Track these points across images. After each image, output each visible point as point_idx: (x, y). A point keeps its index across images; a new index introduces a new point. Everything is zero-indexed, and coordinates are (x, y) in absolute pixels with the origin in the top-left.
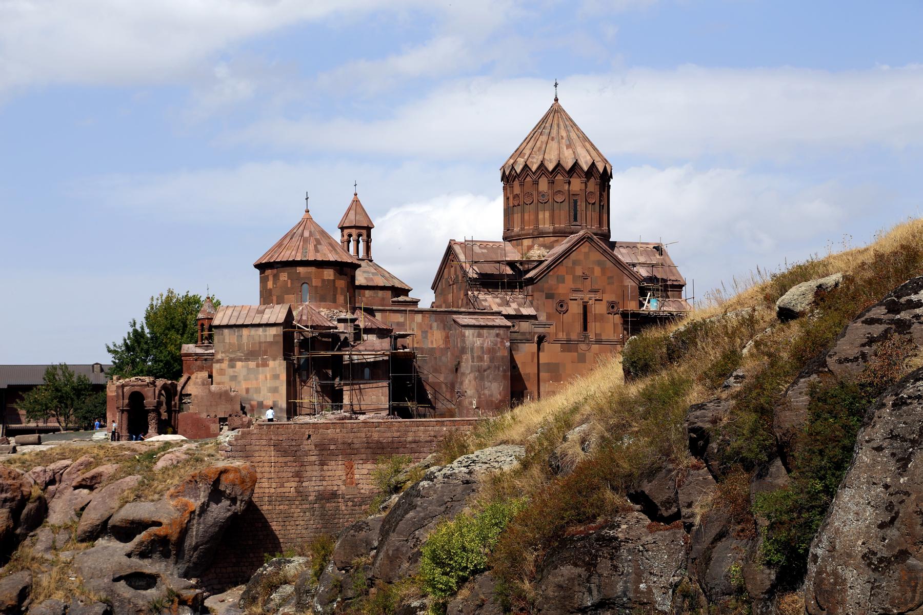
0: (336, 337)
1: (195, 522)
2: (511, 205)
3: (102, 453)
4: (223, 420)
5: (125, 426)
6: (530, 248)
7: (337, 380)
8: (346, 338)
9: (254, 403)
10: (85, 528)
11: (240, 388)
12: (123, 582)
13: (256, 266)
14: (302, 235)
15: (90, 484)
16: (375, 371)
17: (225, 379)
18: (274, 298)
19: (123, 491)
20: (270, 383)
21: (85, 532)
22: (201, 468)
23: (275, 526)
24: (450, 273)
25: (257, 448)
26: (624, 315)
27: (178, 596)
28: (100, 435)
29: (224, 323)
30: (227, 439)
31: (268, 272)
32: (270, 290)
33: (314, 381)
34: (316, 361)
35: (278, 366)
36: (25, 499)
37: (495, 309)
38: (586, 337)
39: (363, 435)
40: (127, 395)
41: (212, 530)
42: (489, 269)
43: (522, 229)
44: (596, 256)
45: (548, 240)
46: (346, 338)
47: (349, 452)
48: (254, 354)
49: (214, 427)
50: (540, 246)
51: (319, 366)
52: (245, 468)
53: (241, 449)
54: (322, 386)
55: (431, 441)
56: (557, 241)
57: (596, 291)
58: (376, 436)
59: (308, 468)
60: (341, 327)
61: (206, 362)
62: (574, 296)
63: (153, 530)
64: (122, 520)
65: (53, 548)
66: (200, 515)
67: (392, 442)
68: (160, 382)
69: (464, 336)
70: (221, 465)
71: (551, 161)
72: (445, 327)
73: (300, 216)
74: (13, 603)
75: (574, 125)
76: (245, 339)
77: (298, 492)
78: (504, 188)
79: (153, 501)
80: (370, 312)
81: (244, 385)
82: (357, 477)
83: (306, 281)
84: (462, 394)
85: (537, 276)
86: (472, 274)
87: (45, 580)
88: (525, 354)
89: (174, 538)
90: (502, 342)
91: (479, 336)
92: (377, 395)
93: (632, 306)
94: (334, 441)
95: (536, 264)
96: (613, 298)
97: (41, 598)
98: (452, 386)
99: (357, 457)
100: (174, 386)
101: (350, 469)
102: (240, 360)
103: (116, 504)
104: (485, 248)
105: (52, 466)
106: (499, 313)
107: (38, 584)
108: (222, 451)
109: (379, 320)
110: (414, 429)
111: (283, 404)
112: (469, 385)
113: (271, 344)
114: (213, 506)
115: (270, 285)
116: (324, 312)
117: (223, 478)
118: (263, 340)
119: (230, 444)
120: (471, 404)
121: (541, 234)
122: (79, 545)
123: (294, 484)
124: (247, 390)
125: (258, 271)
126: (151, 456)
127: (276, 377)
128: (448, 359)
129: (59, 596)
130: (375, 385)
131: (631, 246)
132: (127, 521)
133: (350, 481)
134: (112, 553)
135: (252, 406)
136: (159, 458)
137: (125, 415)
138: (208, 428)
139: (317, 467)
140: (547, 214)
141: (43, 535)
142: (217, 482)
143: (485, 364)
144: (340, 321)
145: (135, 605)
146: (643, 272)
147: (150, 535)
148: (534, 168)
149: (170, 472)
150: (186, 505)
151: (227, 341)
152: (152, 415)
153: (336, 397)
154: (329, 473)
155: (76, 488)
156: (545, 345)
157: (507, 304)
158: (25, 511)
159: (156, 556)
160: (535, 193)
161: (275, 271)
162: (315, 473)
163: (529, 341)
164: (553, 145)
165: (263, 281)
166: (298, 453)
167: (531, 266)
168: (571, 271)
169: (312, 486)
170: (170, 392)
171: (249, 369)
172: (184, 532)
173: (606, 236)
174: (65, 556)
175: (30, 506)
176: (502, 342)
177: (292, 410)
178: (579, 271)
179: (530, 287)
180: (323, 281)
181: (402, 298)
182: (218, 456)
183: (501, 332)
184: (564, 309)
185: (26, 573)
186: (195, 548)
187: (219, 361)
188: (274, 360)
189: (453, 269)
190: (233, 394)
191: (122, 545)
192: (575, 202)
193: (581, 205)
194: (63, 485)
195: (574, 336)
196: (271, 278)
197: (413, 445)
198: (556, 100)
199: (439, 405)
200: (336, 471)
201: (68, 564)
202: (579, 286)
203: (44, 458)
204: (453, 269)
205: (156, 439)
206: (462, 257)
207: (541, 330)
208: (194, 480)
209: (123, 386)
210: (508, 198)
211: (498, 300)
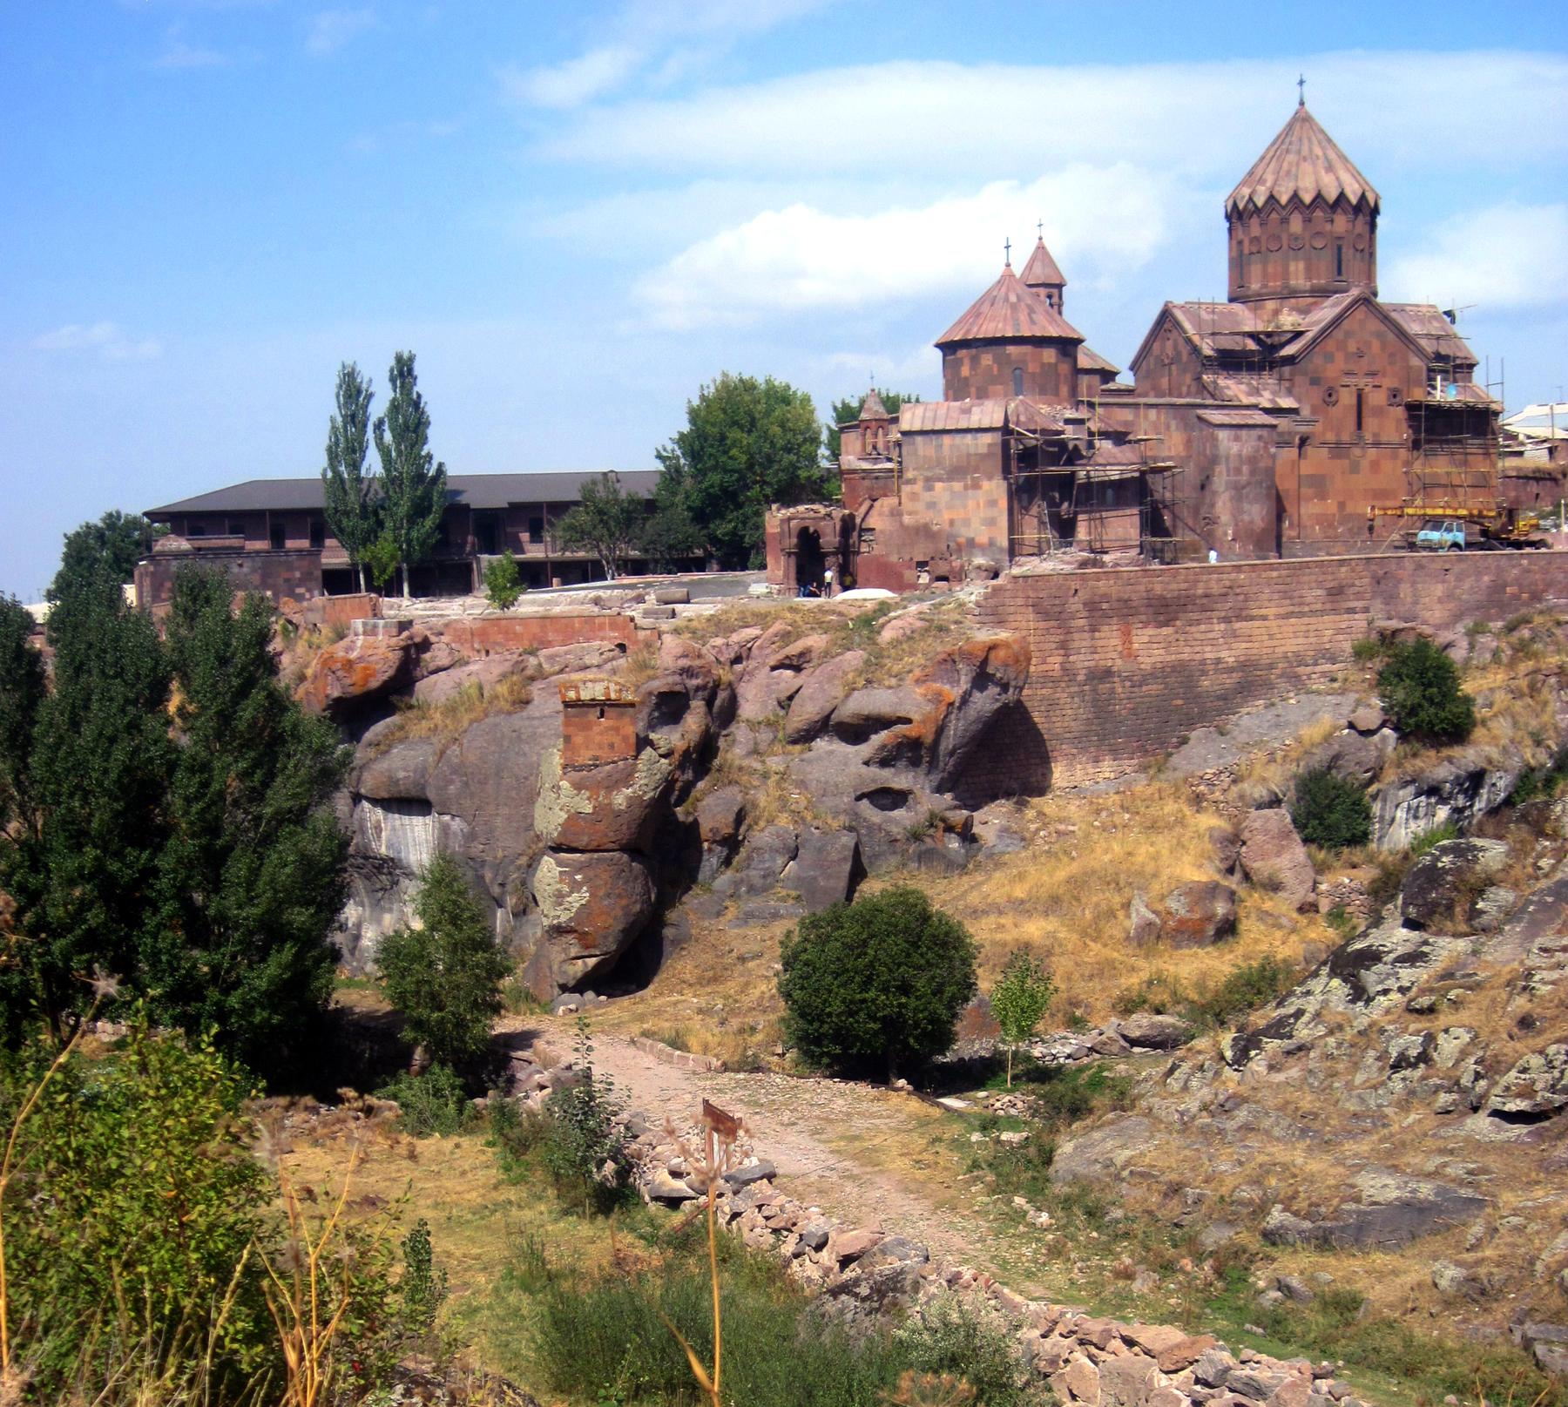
0: (1062, 444)
1: (953, 717)
2: (1246, 251)
3: (798, 617)
4: (922, 565)
5: (793, 574)
6: (1276, 312)
7: (1066, 505)
8: (1076, 447)
9: (961, 540)
10: (800, 726)
11: (940, 520)
12: (865, 801)
13: (938, 346)
14: (1007, 299)
17: (920, 506)
18: (973, 390)
19: (845, 673)
20: (984, 513)
21: (799, 731)
23: (1037, 718)
25: (1012, 609)
26: (1413, 408)
27: (943, 820)
29: (917, 427)
30: (973, 598)
31: (962, 353)
32: (966, 379)
33: (1039, 508)
34: (1045, 480)
35: (996, 488)
36: (717, 685)
37: (1246, 400)
38: (1361, 437)
39: (1142, 588)
40: (794, 532)
41: (973, 727)
43: (1264, 286)
44: (1374, 325)
45: (1303, 302)
46: (1076, 447)
47: (1125, 611)
48: (959, 471)
50: (1292, 309)
52: (1015, 641)
53: (993, 612)
54: (1050, 515)
55: (1225, 595)
56: (1315, 304)
57: (1373, 374)
58: (1158, 589)
59: (1076, 636)
60: (1070, 433)
62: (1346, 380)
63: (900, 729)
64: (855, 715)
65: (755, 752)
66: (960, 708)
67: (1179, 597)
69: (1216, 439)
70: (984, 636)
71: (1306, 190)
72: (1187, 427)
74: (730, 831)
75: (1329, 140)
76: (946, 451)
77: (1064, 669)
78: (1230, 230)
79: (890, 687)
81: (946, 516)
82: (1136, 646)
83: (1019, 368)
84: (1212, 521)
85: (1300, 352)
87: (762, 800)
89: (929, 739)
90: (1266, 448)
91: (1237, 439)
92: (1124, 525)
93: (1418, 395)
94: (1106, 597)
95: (1289, 336)
96: (1395, 384)
97: (762, 824)
98: (1196, 510)
99: (1135, 619)
100: (852, 517)
101: (1127, 635)
102: (940, 480)
103: (839, 692)
104: (1213, 312)
105: (735, 638)
106: (1255, 407)
107: (755, 805)
110: (1205, 577)
111: (1004, 542)
112: (1223, 508)
113: (984, 457)
114: (977, 695)
115: (965, 371)
117: (992, 655)
118: (972, 451)
119: (978, 605)
120: (1226, 534)
121: (1293, 294)
122: (790, 747)
123: (1059, 659)
124: (952, 522)
125: (939, 354)
127: (992, 503)
128: (1191, 472)
129: (784, 820)
130: (1120, 513)
131: (1401, 308)
132: (858, 716)
133: (1129, 655)
135: (959, 545)
136: (883, 626)
137: (793, 560)
138: (900, 576)
139: (1086, 635)
140: (1301, 265)
141: (740, 731)
142: (985, 662)
143: (1244, 478)
144: (1068, 421)
145: (888, 833)
147: (897, 737)
148: (1284, 199)
149: (905, 646)
150: (939, 693)
151: (921, 452)
152: (830, 560)
153: (1065, 530)
154: (1101, 643)
155: (774, 668)
156: (1309, 450)
157: (1256, 392)
158: (718, 703)
159: (901, 764)
160: (1285, 238)
161: (974, 351)
162: (1084, 644)
163: (1288, 444)
165: (950, 368)
166: (1063, 616)
167: (1283, 339)
168: (1341, 346)
169: (1082, 661)
171: (953, 492)
172: (940, 731)
174: (775, 763)
175: (722, 695)
176: (1266, 448)
177: (1013, 551)
178: (1352, 347)
179: (1287, 370)
180: (1043, 365)
181: (1111, 386)
182: (967, 623)
183: (1264, 433)
184: (1333, 398)
185: (736, 789)
186: (951, 754)
187: (909, 482)
188: (990, 478)
189: (1169, 344)
190: (935, 528)
191: (850, 749)
192: (1340, 248)
193: (1348, 253)
194: (752, 664)
195: (1346, 438)
196: (967, 362)
197: (1205, 601)
198: (1302, 104)
200: (1110, 636)
201: (783, 776)
202: (1351, 367)
203: (719, 625)
204: (1169, 344)
206: (1187, 325)
207: (1303, 429)
208: (950, 660)
209: (790, 519)
210: (1240, 243)
211: (1243, 387)
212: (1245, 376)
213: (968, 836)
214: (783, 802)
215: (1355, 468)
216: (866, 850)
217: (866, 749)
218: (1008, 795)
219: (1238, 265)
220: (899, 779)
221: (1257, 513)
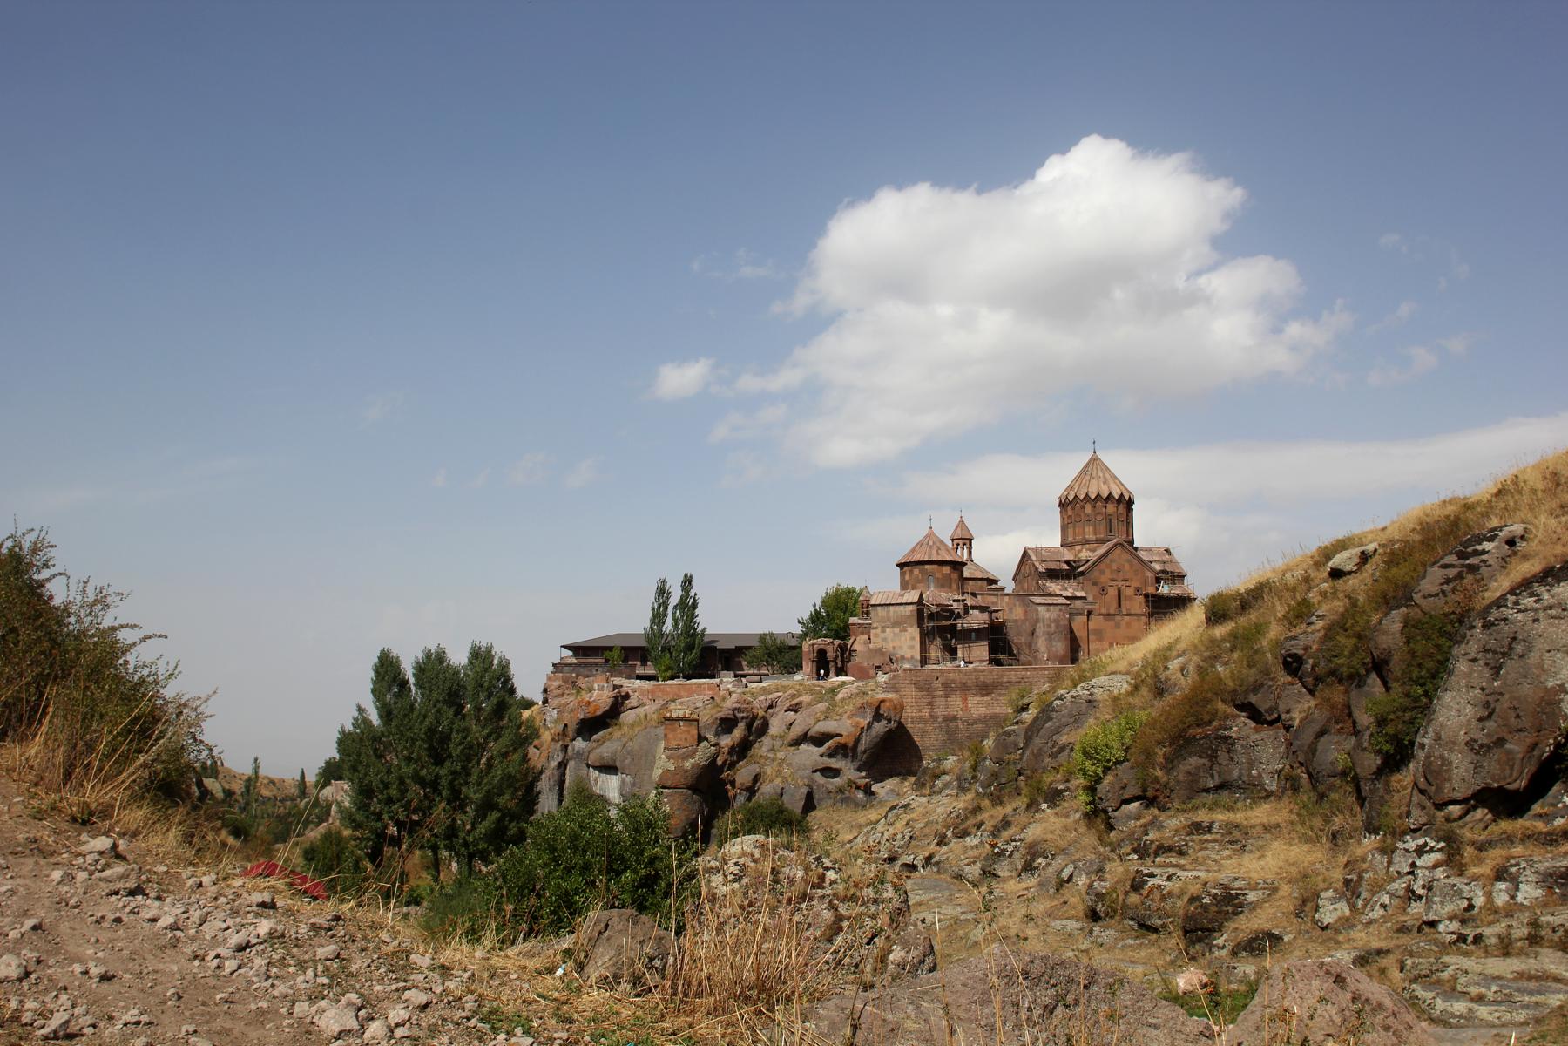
0: (952, 612)
11: (888, 647)
15: (795, 709)
16: (979, 634)
20: (909, 643)
22: (867, 698)
24: (1026, 569)
26: (1146, 596)
28: (798, 677)
33: (938, 641)
34: (940, 628)
35: (914, 632)
42: (1053, 566)
44: (1126, 556)
48: (898, 623)
49: (873, 672)
51: (940, 631)
60: (955, 605)
61: (866, 629)
65: (773, 749)
68: (837, 642)
70: (881, 696)
72: (1024, 605)
73: (926, 531)
80: (974, 595)
84: (1037, 651)
86: (1041, 569)
88: (1079, 623)
92: (981, 650)
93: (1151, 590)
96: (1138, 584)
98: (1030, 645)
108: (879, 687)
109: (980, 601)
112: (1041, 644)
116: (944, 595)
126: (833, 691)
128: (1027, 627)
134: (810, 754)
142: (878, 708)
146: (1158, 567)
153: (953, 652)
164: (1094, 482)
165: (902, 575)
168: (1109, 566)
170: (843, 648)
172: (857, 741)
173: (1131, 543)
174: (780, 755)
177: (924, 661)
193: (1114, 522)
199: (1022, 658)
201: (783, 760)
203: (765, 691)
205: (835, 680)
208: (862, 707)
212: (1061, 582)
213: (868, 792)
214: (779, 772)
215: (1118, 626)
216: (816, 796)
217: (822, 750)
218: (898, 775)
219: (1064, 529)
220: (835, 763)
221: (1061, 647)
